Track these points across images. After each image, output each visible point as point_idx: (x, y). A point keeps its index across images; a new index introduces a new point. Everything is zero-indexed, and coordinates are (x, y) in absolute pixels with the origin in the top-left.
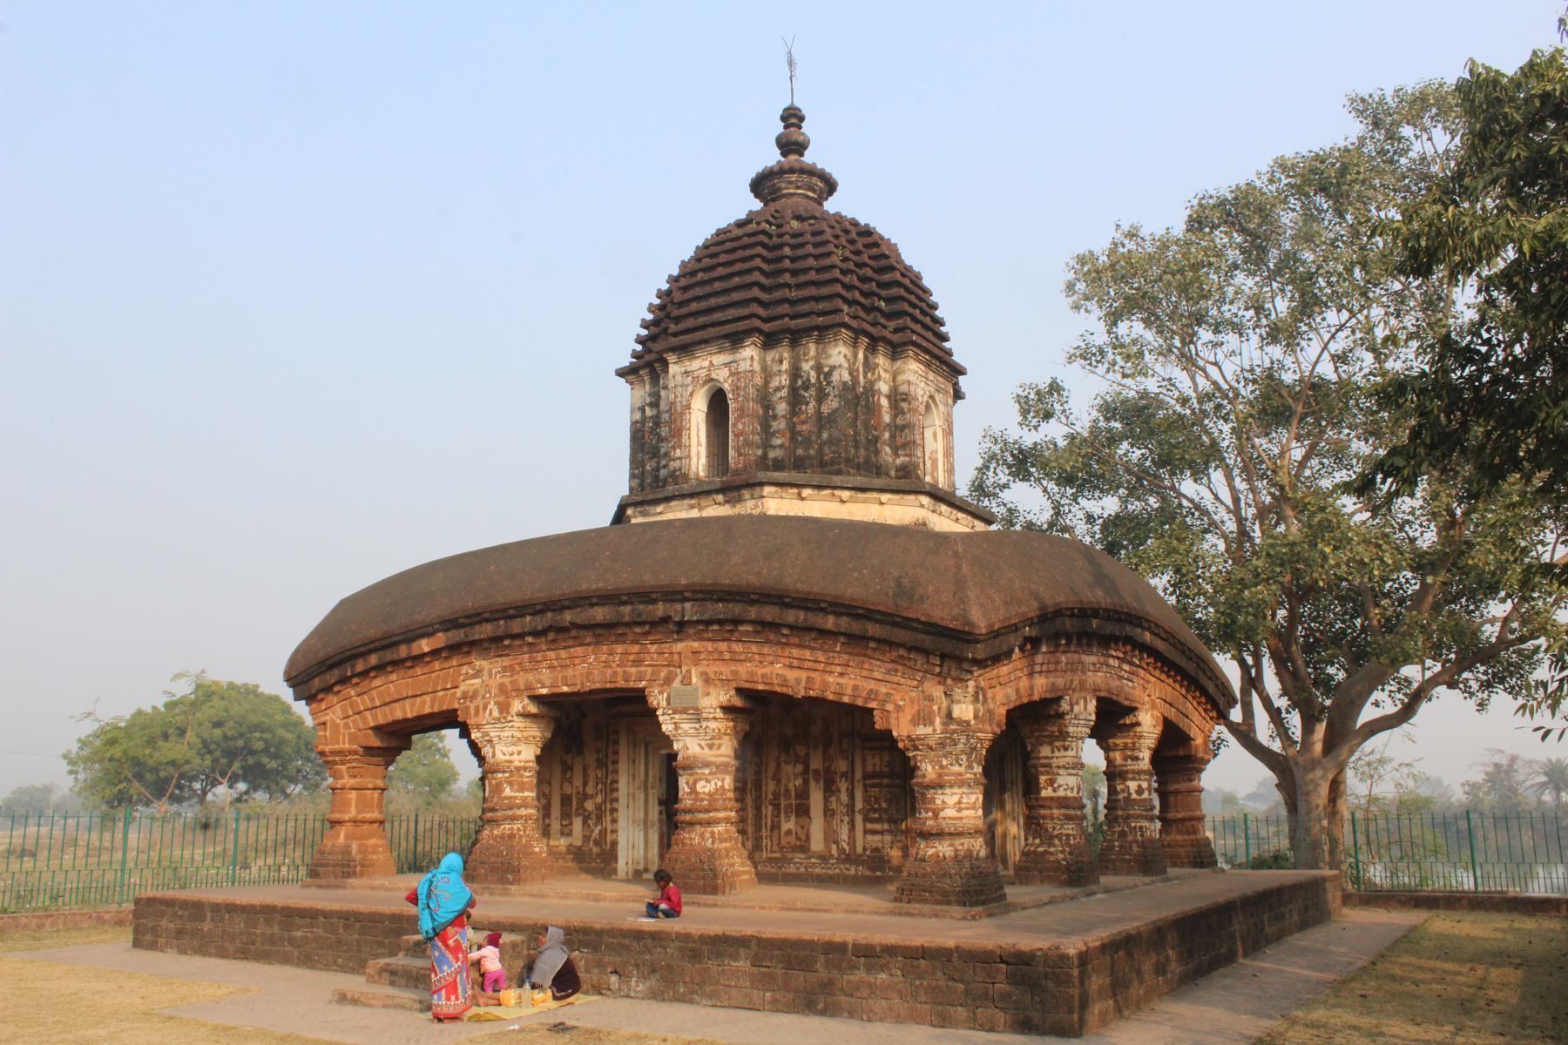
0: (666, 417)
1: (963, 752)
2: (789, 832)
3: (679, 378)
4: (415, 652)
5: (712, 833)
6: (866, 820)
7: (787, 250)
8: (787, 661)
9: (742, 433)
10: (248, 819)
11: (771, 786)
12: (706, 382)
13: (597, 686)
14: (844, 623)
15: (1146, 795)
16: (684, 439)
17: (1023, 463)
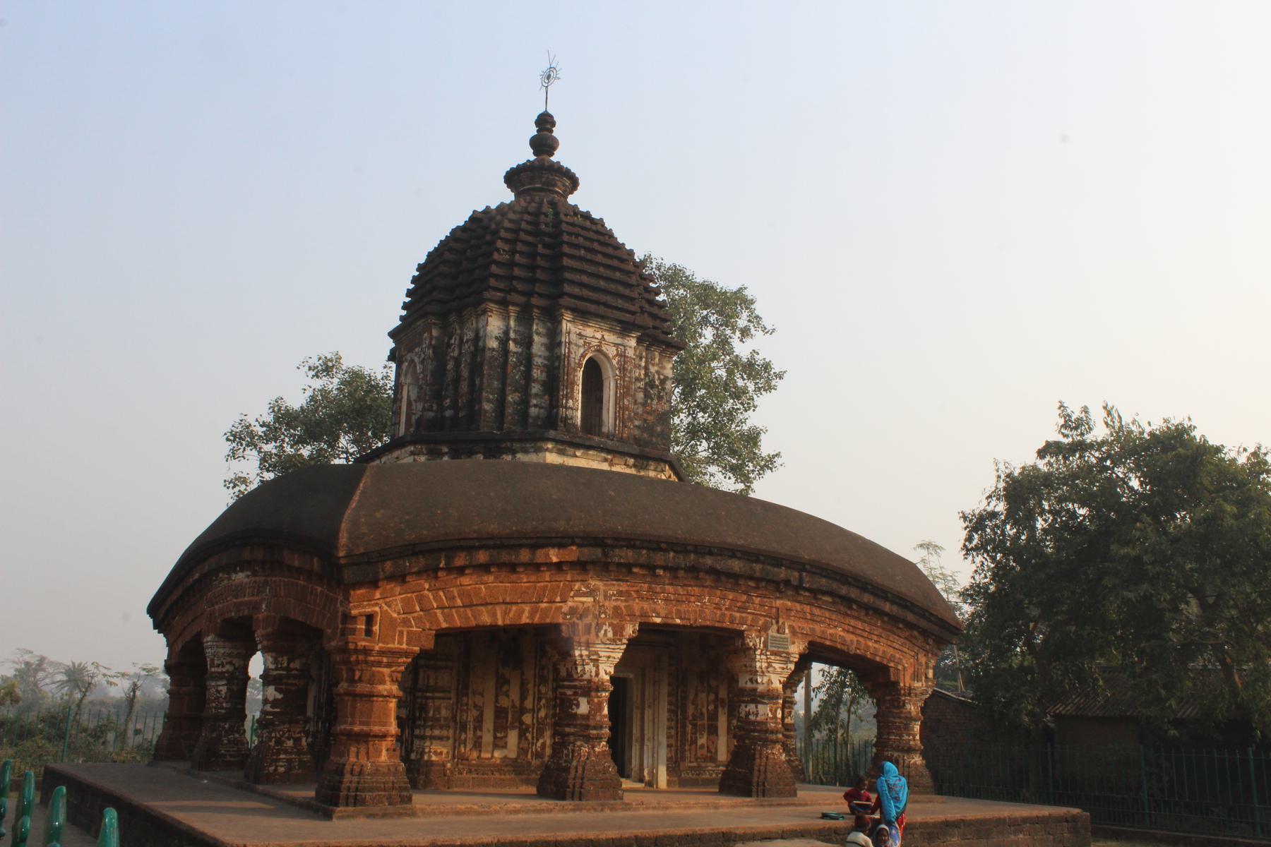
2: (702, 746)
14: (895, 610)
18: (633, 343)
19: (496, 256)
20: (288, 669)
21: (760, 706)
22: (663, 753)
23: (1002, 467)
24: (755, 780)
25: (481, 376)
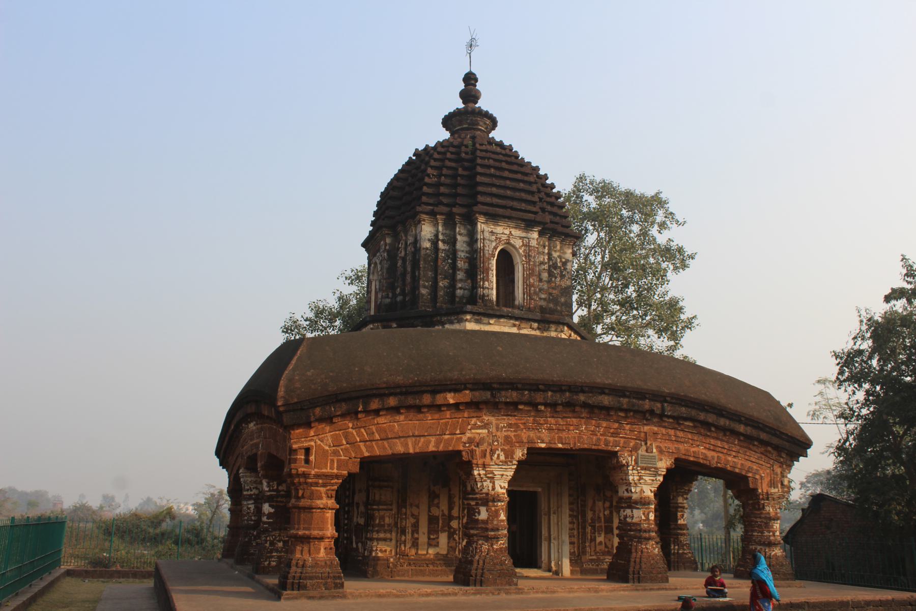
2: (600, 543)
8: (708, 446)
13: (586, 446)
18: (535, 235)
19: (427, 180)
20: (277, 490)
21: (634, 511)
22: (566, 549)
23: (863, 313)
24: (631, 569)
25: (419, 269)
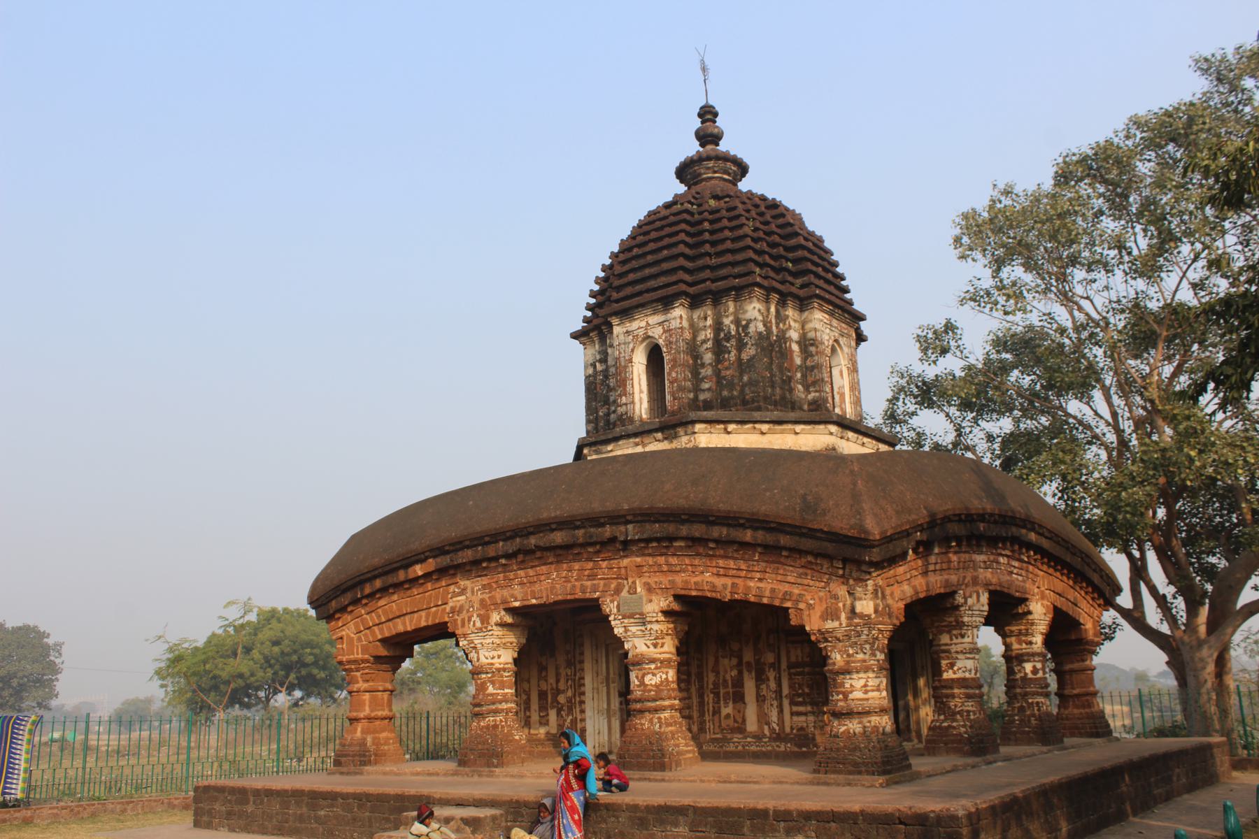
0: (612, 370)
1: (866, 642)
2: (728, 716)
3: (622, 337)
4: (411, 576)
5: (659, 718)
6: (792, 703)
7: (706, 224)
8: (715, 570)
9: (676, 380)
10: (304, 720)
11: (712, 677)
12: (644, 340)
13: (560, 598)
14: (760, 536)
15: (1040, 674)
16: (629, 388)
17: (928, 393)
